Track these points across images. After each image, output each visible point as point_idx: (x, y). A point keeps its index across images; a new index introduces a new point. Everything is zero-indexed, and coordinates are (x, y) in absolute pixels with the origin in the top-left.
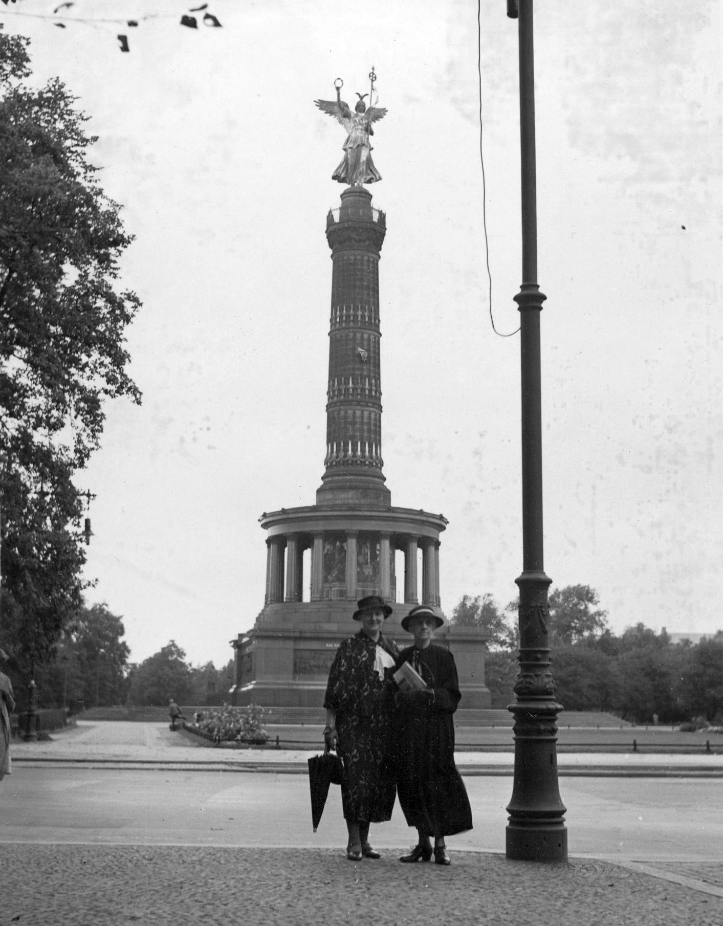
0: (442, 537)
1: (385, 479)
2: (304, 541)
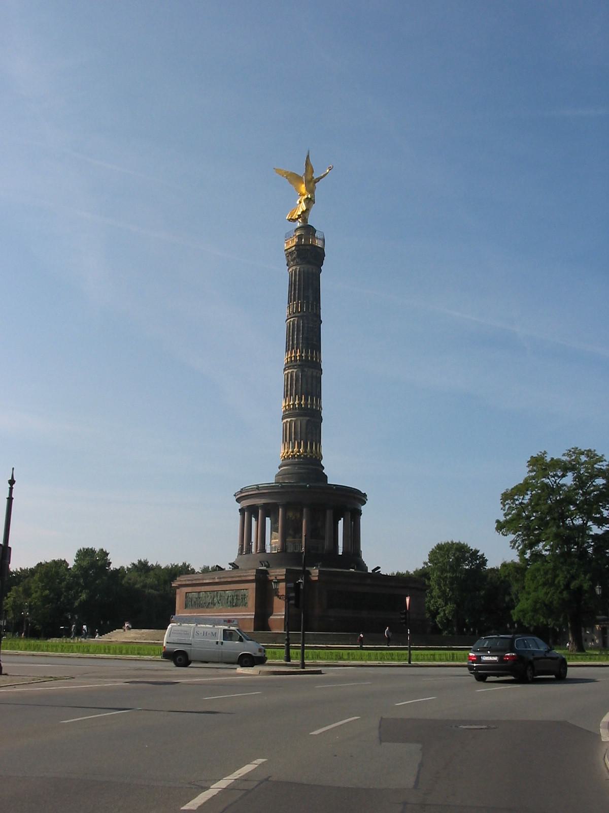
1: (323, 468)
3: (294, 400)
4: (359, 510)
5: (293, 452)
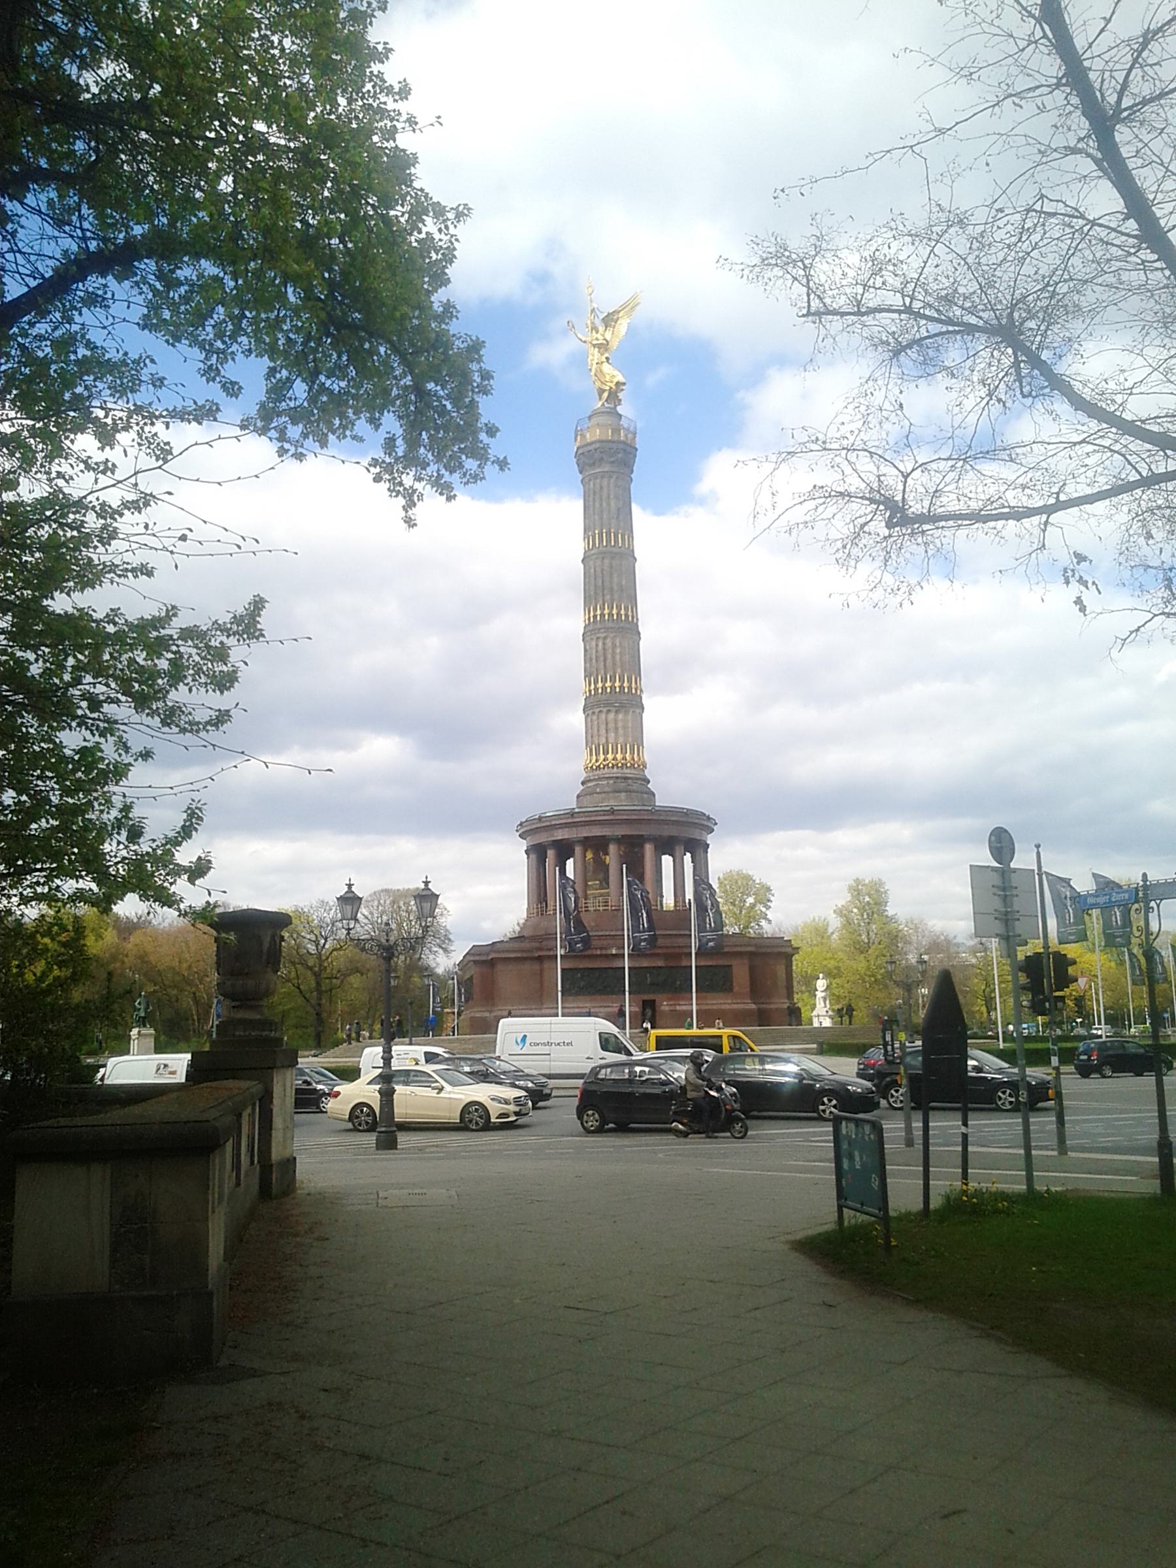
0: (710, 839)
2: (564, 850)
5: (597, 761)
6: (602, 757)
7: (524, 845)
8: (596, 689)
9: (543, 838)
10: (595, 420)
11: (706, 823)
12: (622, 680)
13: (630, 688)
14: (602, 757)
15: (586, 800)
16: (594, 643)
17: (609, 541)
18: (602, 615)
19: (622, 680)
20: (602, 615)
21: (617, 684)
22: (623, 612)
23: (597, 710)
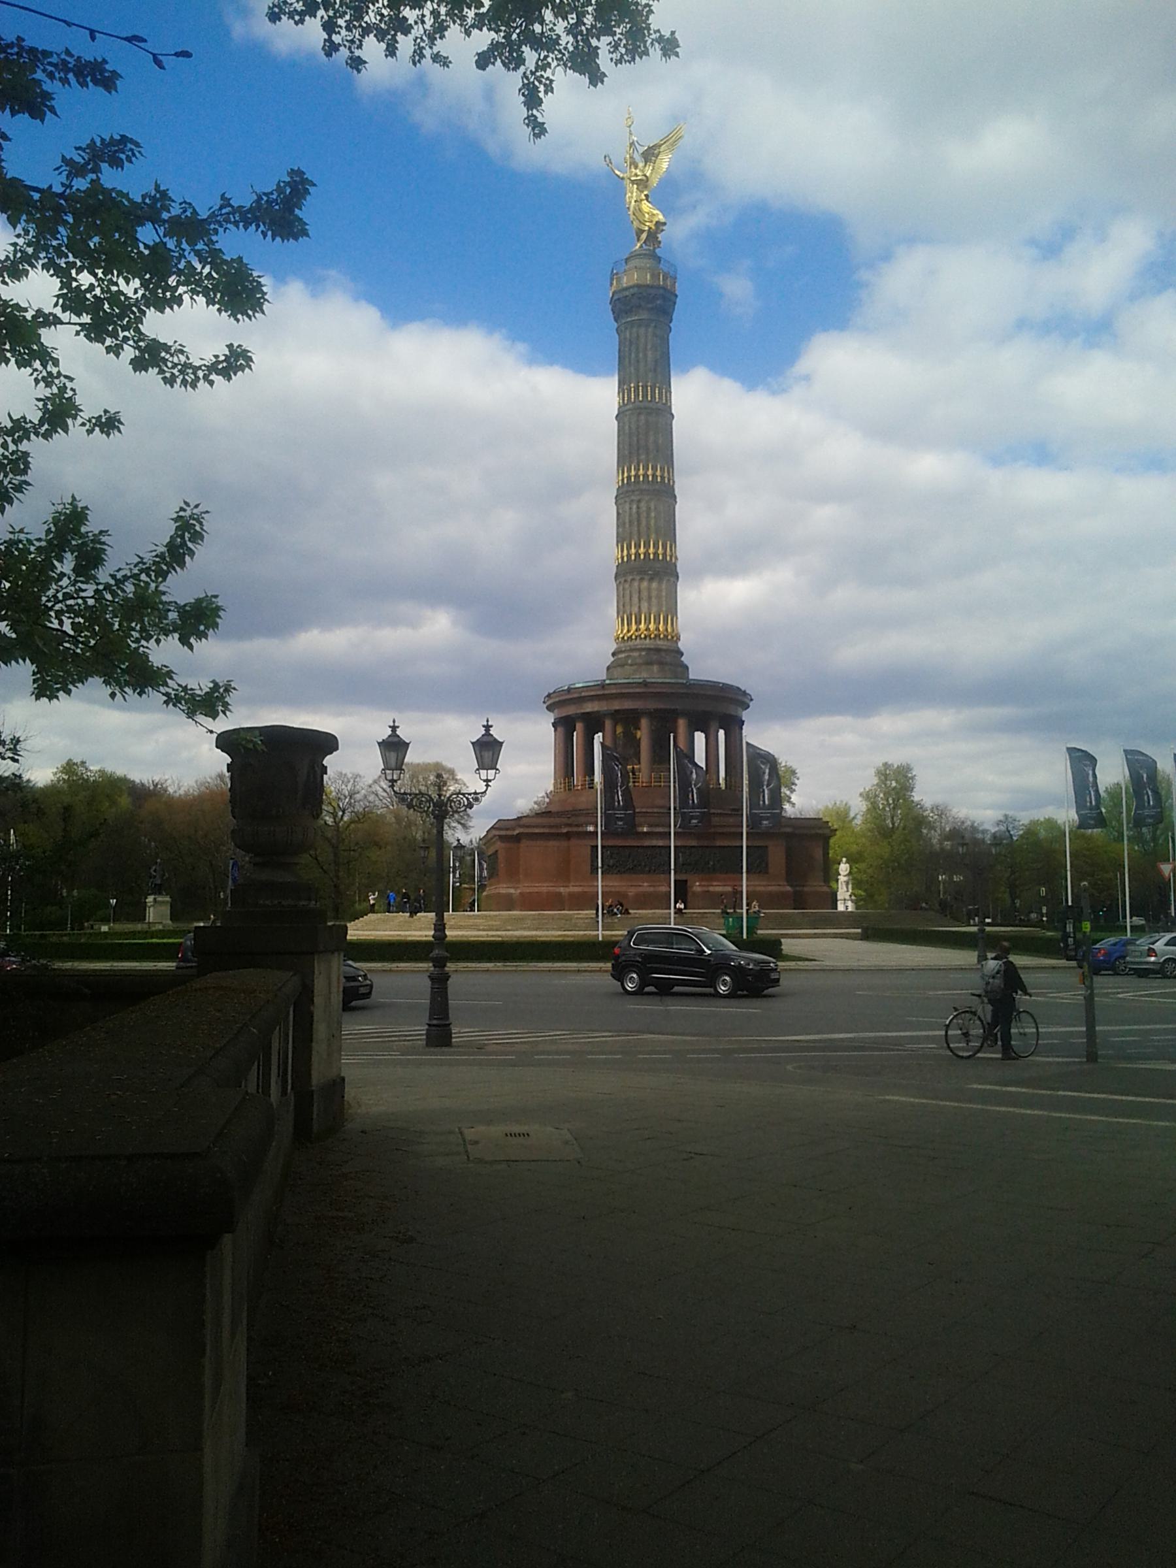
0: (745, 715)
2: (593, 724)
3: (629, 548)
4: (731, 716)
5: (628, 631)
6: (634, 627)
7: (551, 718)
8: (629, 555)
9: (571, 710)
10: (633, 263)
11: (740, 698)
12: (656, 546)
13: (664, 554)
14: (634, 627)
15: (617, 672)
16: (627, 507)
17: (645, 395)
18: (637, 476)
19: (656, 546)
20: (637, 476)
21: (651, 550)
22: (658, 473)
23: (629, 578)
